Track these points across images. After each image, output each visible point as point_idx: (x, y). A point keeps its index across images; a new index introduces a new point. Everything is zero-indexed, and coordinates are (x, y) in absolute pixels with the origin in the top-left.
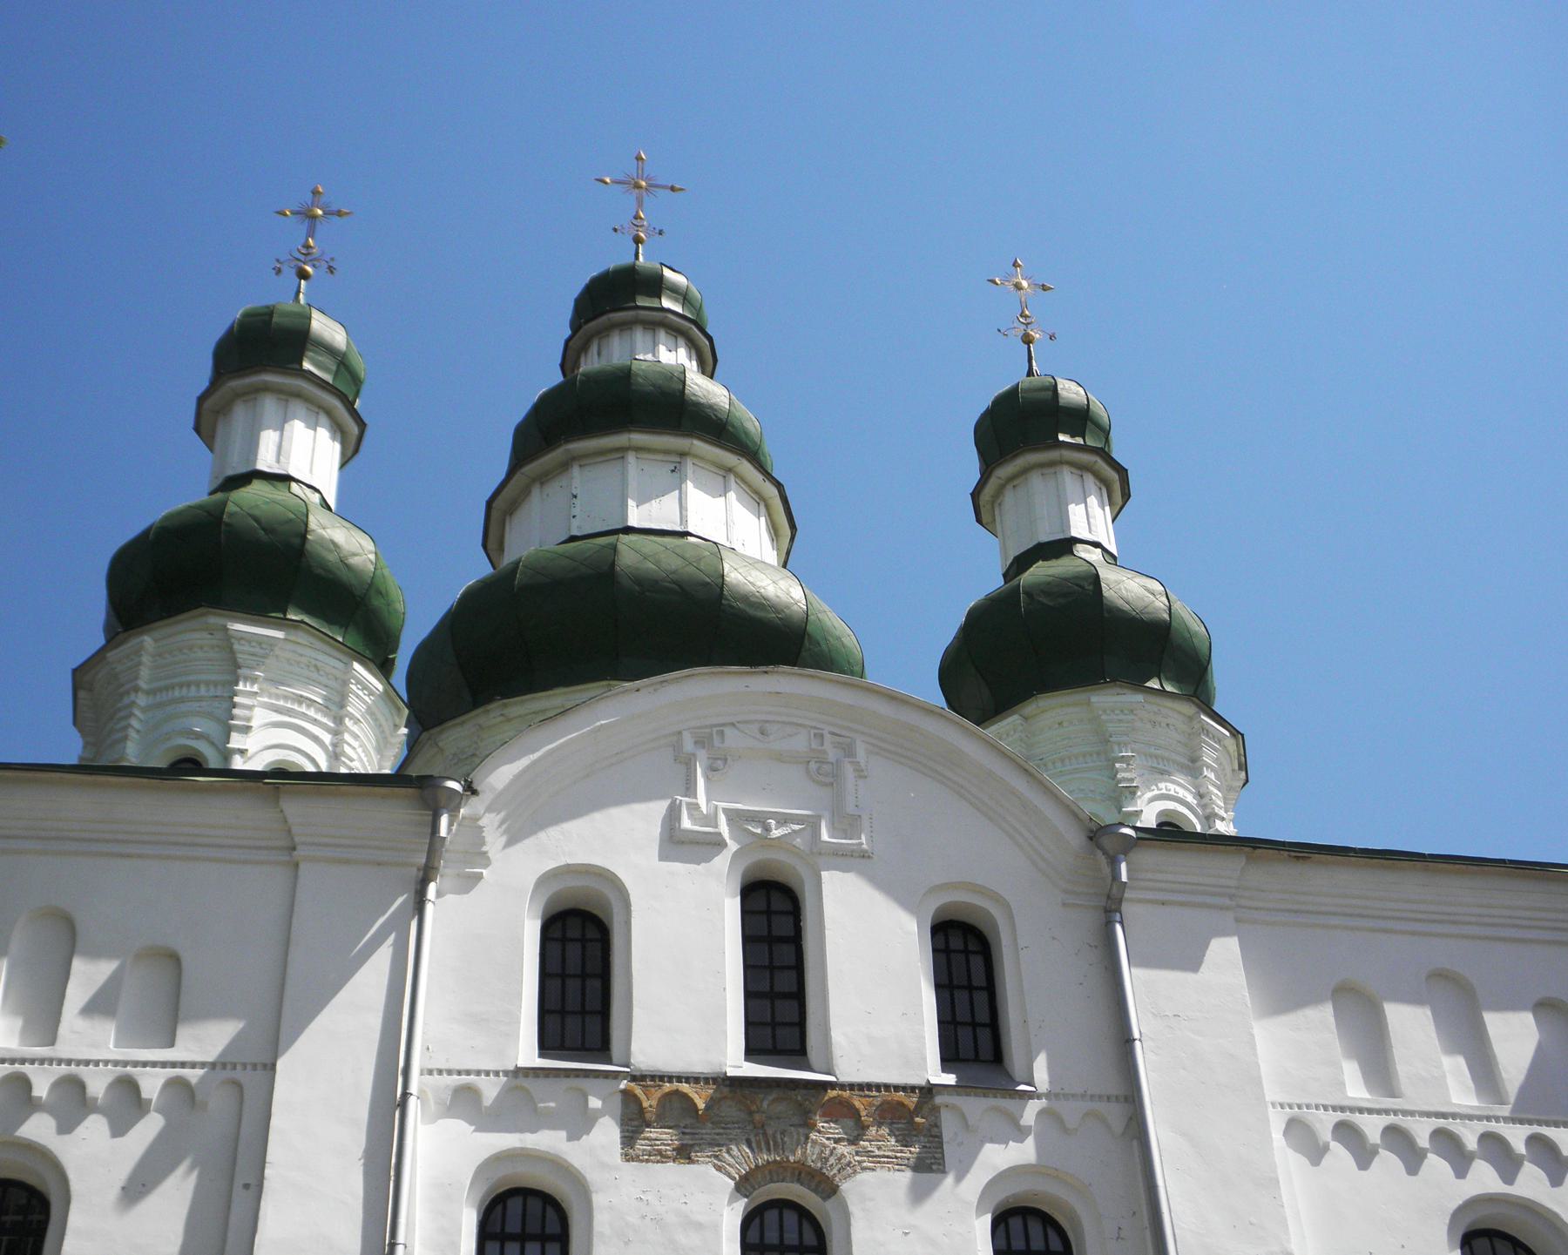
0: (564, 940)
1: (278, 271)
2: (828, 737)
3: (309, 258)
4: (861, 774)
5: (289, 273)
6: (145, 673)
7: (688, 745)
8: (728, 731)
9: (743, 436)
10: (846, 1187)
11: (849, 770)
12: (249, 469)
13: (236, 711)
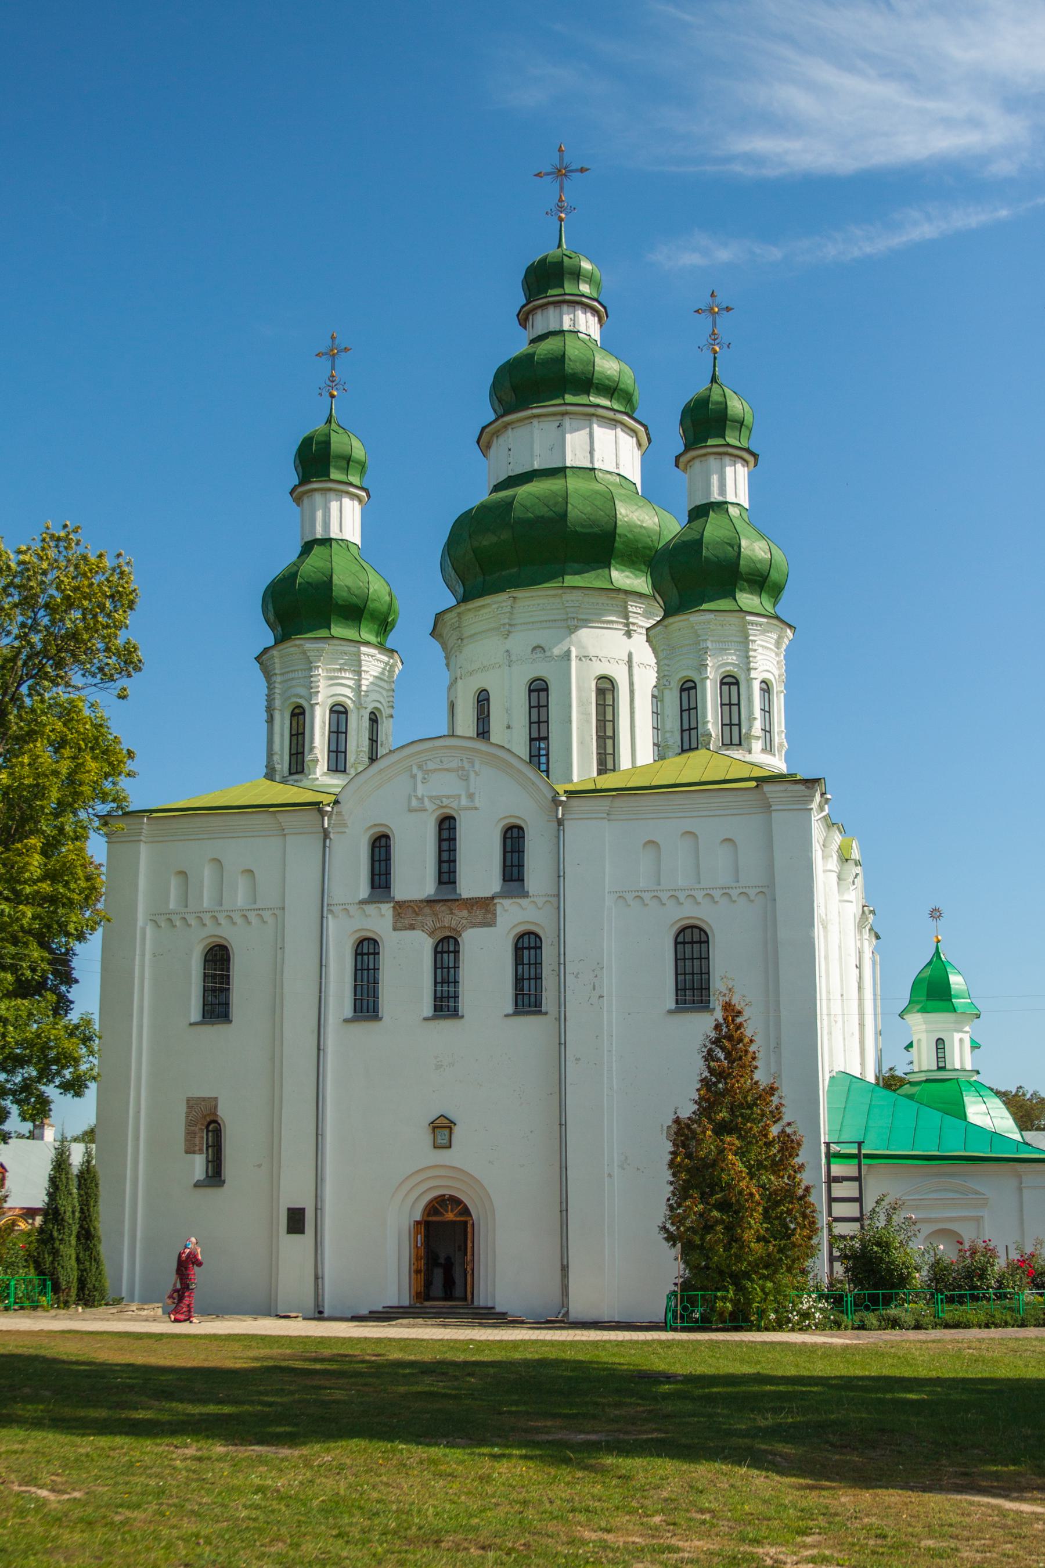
0: (380, 847)
1: (321, 394)
2: (465, 759)
3: (334, 384)
4: (477, 774)
5: (326, 395)
6: (277, 666)
7: (415, 770)
8: (429, 762)
9: (607, 382)
10: (464, 935)
11: (472, 775)
12: (313, 538)
13: (313, 685)
